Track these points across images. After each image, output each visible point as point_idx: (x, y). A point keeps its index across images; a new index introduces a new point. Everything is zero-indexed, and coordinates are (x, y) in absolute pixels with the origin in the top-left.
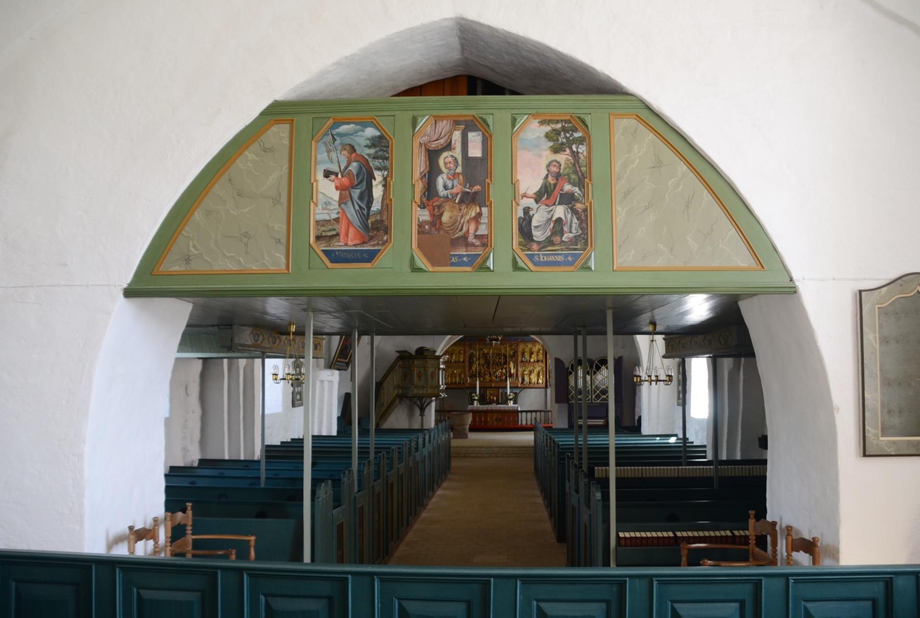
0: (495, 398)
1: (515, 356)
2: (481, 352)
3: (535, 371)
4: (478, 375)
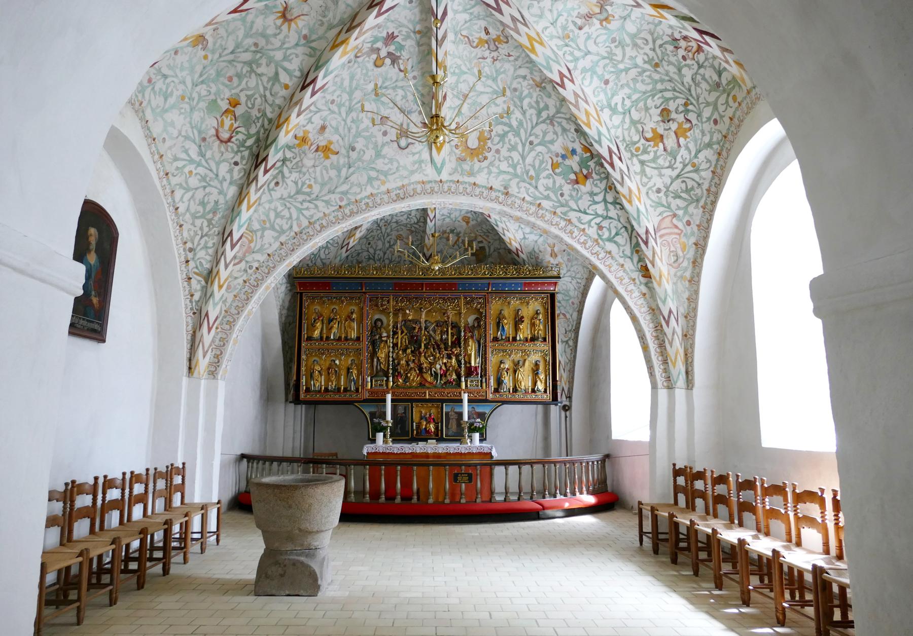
0: (432, 427)
1: (479, 326)
2: (400, 319)
3: (527, 363)
4: (391, 371)
